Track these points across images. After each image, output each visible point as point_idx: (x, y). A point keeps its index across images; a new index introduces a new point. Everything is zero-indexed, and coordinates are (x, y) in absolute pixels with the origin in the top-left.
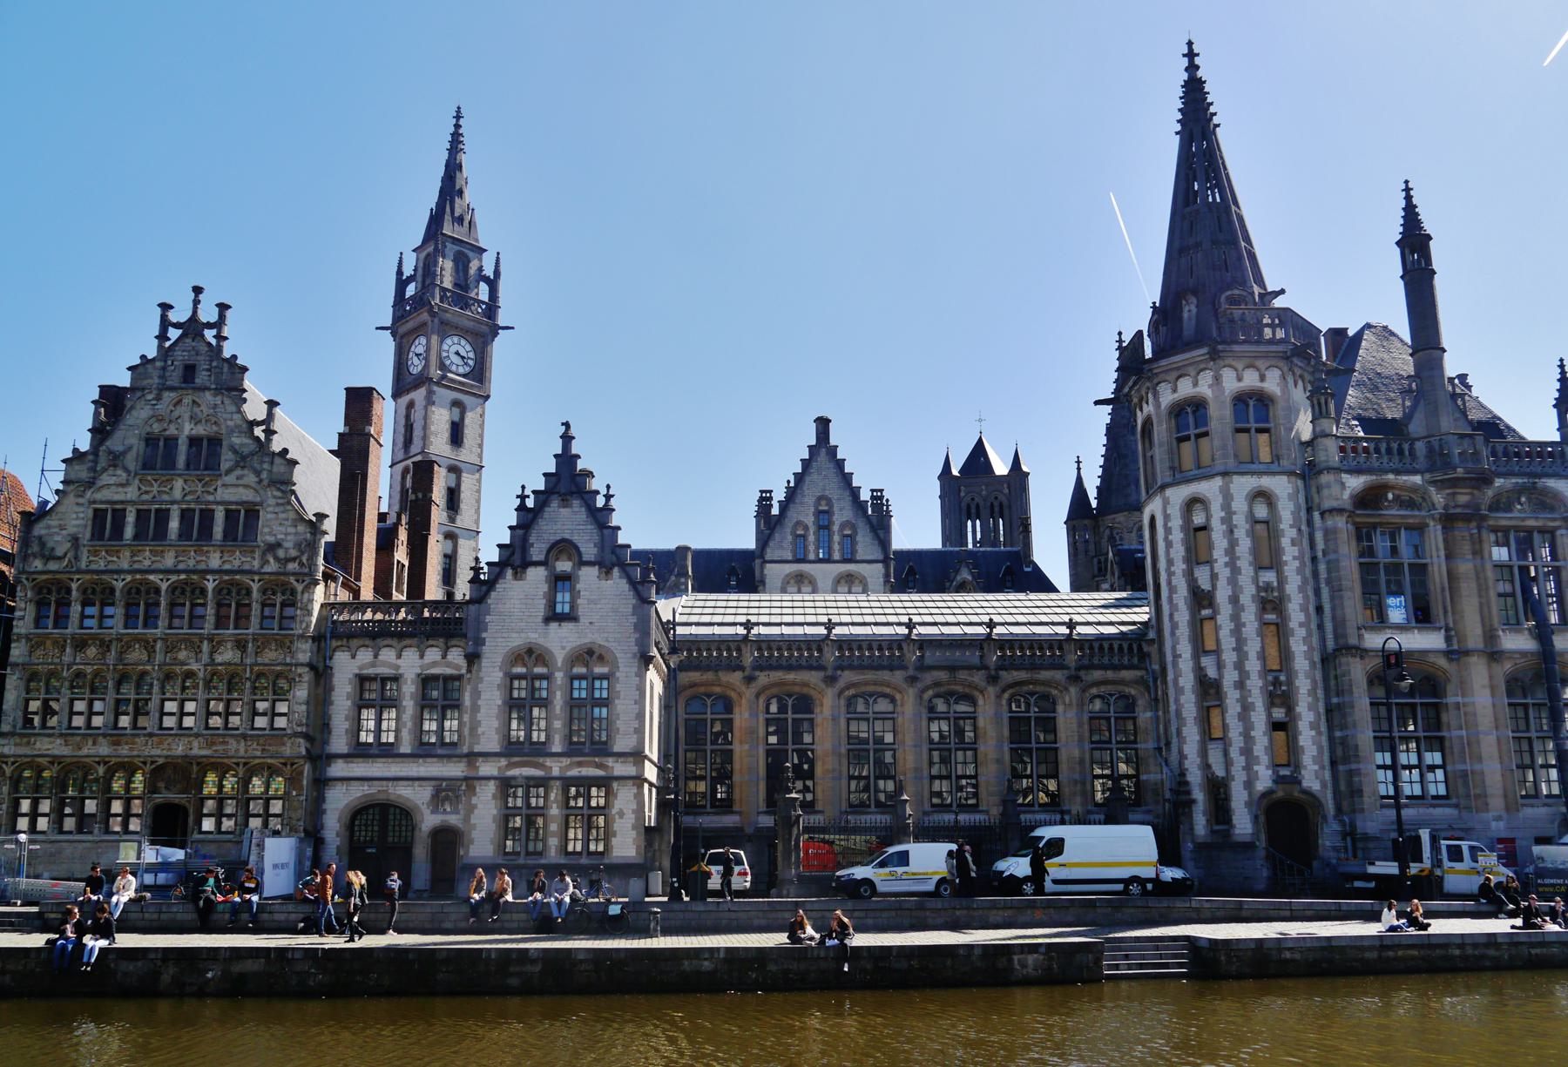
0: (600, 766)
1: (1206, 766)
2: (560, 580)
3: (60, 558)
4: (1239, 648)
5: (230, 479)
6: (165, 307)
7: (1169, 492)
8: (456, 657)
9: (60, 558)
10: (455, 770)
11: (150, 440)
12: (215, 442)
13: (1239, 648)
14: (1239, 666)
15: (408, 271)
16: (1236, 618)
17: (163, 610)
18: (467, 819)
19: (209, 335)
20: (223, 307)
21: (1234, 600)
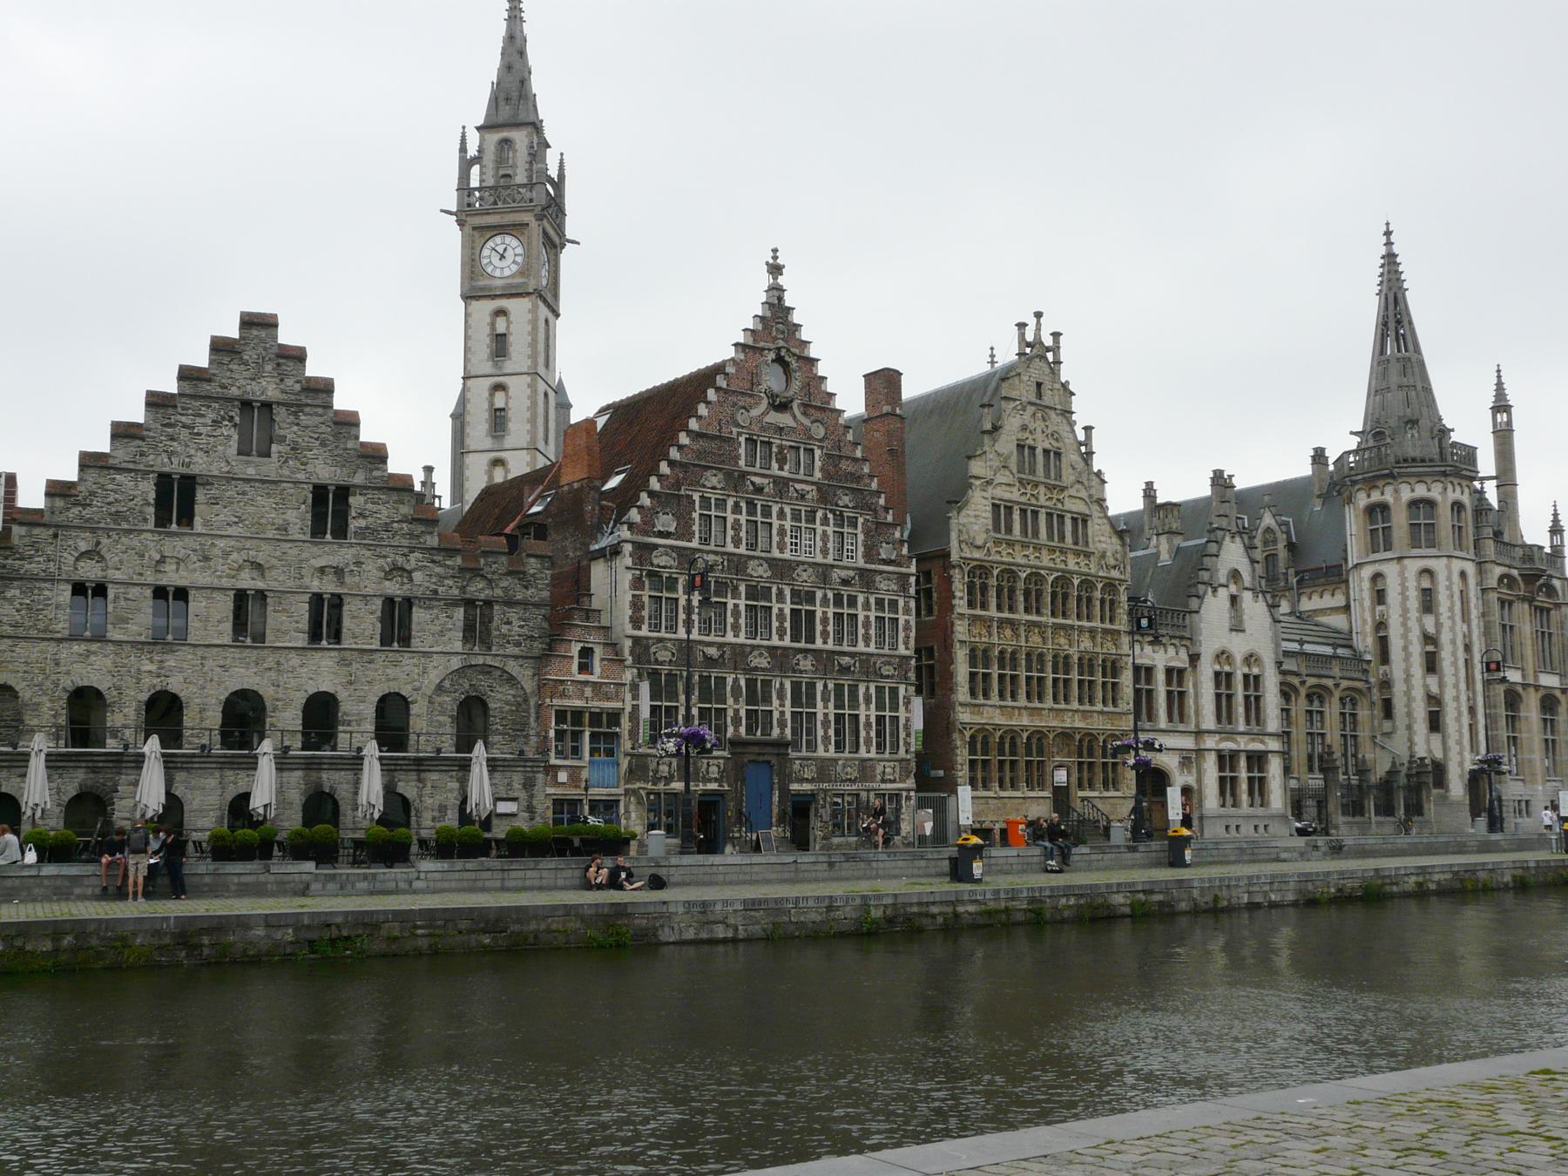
0: (1262, 742)
1: (1430, 751)
2: (1234, 600)
3: (978, 547)
4: (1456, 675)
5: (1072, 492)
6: (1022, 326)
7: (1406, 562)
8: (1183, 654)
9: (978, 547)
10: (1188, 743)
11: (1020, 447)
12: (1058, 455)
13: (1456, 675)
14: (1456, 686)
15: (472, 151)
16: (1454, 654)
17: (993, 593)
18: (1199, 780)
19: (1050, 356)
20: (1056, 335)
21: (1453, 642)
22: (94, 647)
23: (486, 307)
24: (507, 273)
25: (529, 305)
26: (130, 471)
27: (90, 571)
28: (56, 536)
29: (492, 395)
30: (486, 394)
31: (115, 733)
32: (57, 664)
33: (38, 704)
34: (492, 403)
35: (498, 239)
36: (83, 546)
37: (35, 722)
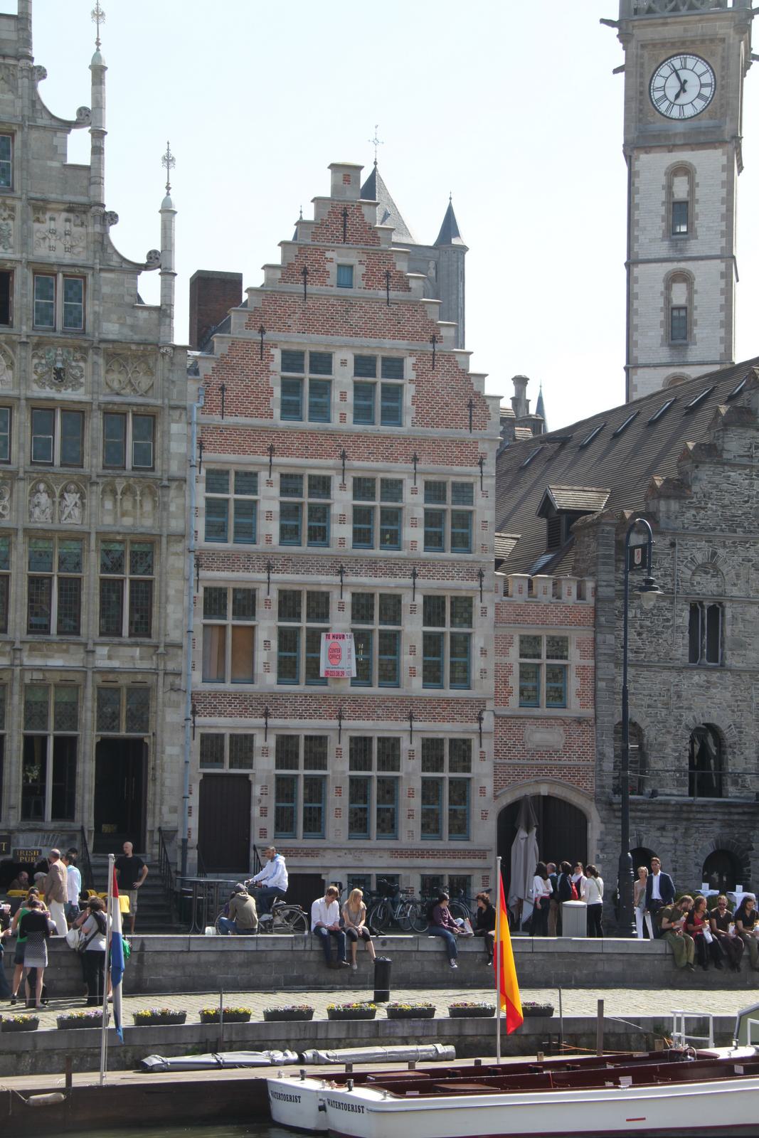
22: (715, 677)
23: (657, 163)
24: (689, 111)
25: (724, 160)
26: (745, 467)
27: (706, 586)
28: (673, 545)
29: (668, 288)
30: (661, 287)
31: (737, 779)
32: (679, 697)
33: (663, 744)
34: (668, 300)
35: (677, 63)
36: (700, 558)
37: (659, 765)
